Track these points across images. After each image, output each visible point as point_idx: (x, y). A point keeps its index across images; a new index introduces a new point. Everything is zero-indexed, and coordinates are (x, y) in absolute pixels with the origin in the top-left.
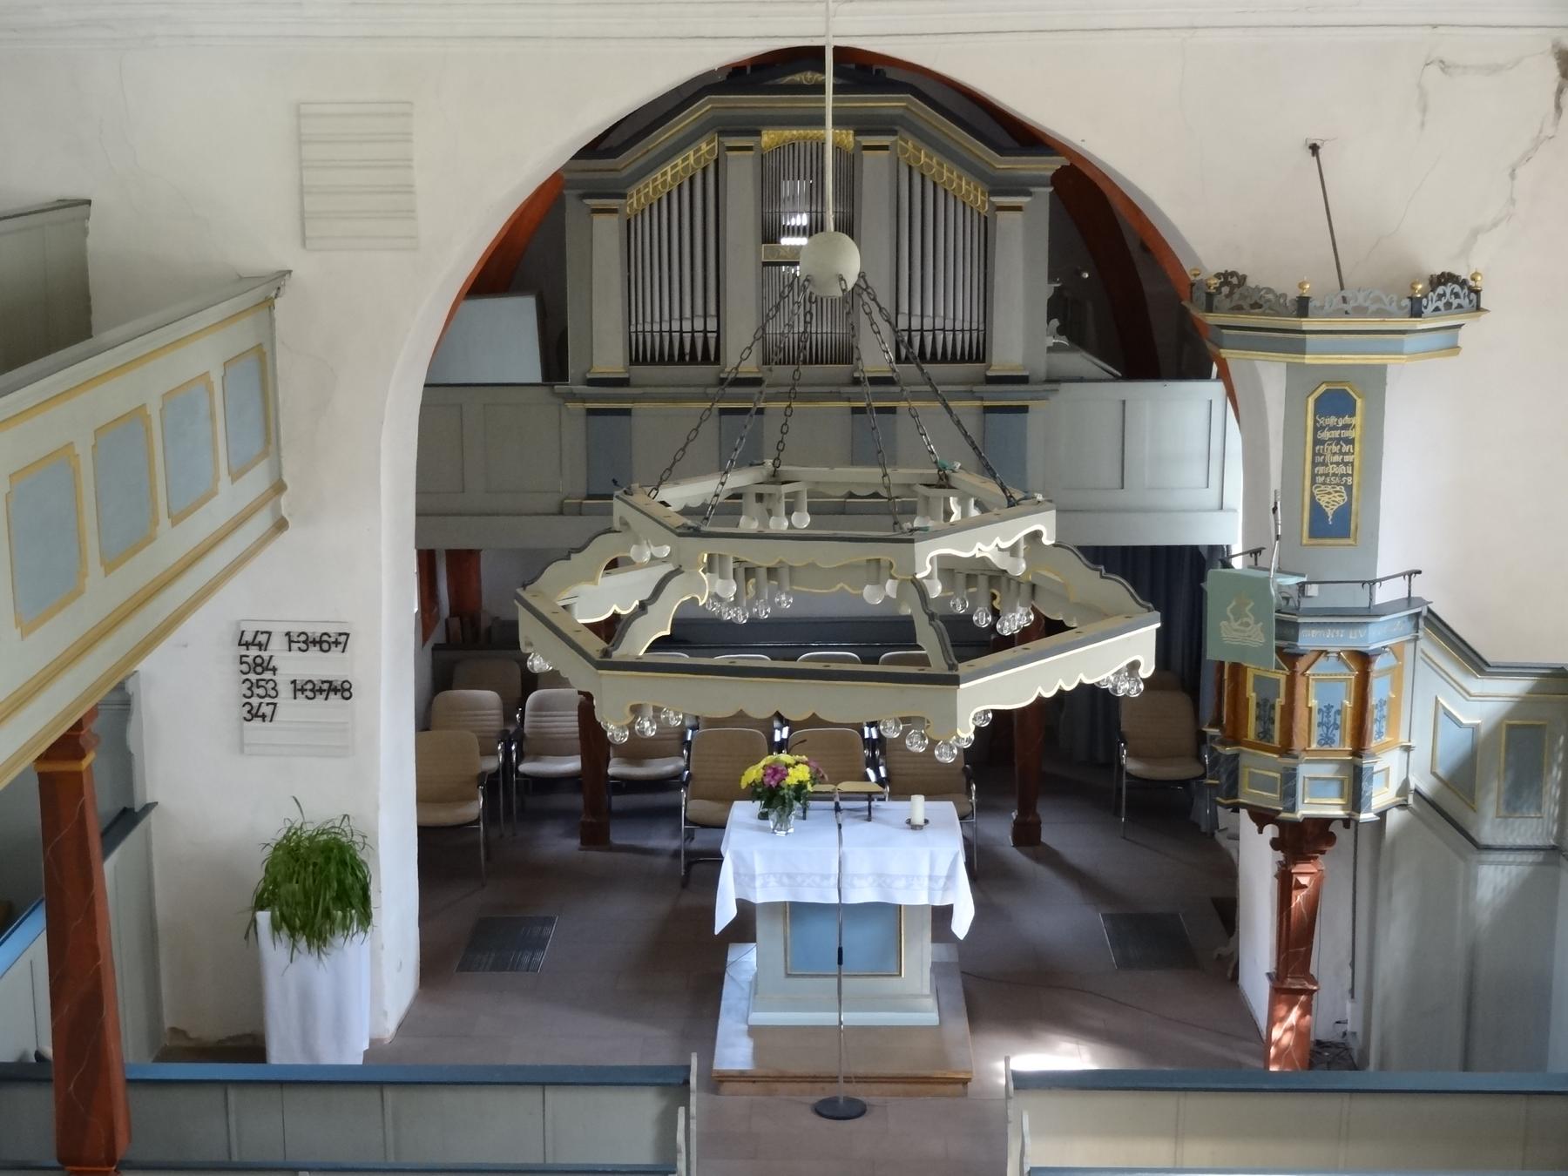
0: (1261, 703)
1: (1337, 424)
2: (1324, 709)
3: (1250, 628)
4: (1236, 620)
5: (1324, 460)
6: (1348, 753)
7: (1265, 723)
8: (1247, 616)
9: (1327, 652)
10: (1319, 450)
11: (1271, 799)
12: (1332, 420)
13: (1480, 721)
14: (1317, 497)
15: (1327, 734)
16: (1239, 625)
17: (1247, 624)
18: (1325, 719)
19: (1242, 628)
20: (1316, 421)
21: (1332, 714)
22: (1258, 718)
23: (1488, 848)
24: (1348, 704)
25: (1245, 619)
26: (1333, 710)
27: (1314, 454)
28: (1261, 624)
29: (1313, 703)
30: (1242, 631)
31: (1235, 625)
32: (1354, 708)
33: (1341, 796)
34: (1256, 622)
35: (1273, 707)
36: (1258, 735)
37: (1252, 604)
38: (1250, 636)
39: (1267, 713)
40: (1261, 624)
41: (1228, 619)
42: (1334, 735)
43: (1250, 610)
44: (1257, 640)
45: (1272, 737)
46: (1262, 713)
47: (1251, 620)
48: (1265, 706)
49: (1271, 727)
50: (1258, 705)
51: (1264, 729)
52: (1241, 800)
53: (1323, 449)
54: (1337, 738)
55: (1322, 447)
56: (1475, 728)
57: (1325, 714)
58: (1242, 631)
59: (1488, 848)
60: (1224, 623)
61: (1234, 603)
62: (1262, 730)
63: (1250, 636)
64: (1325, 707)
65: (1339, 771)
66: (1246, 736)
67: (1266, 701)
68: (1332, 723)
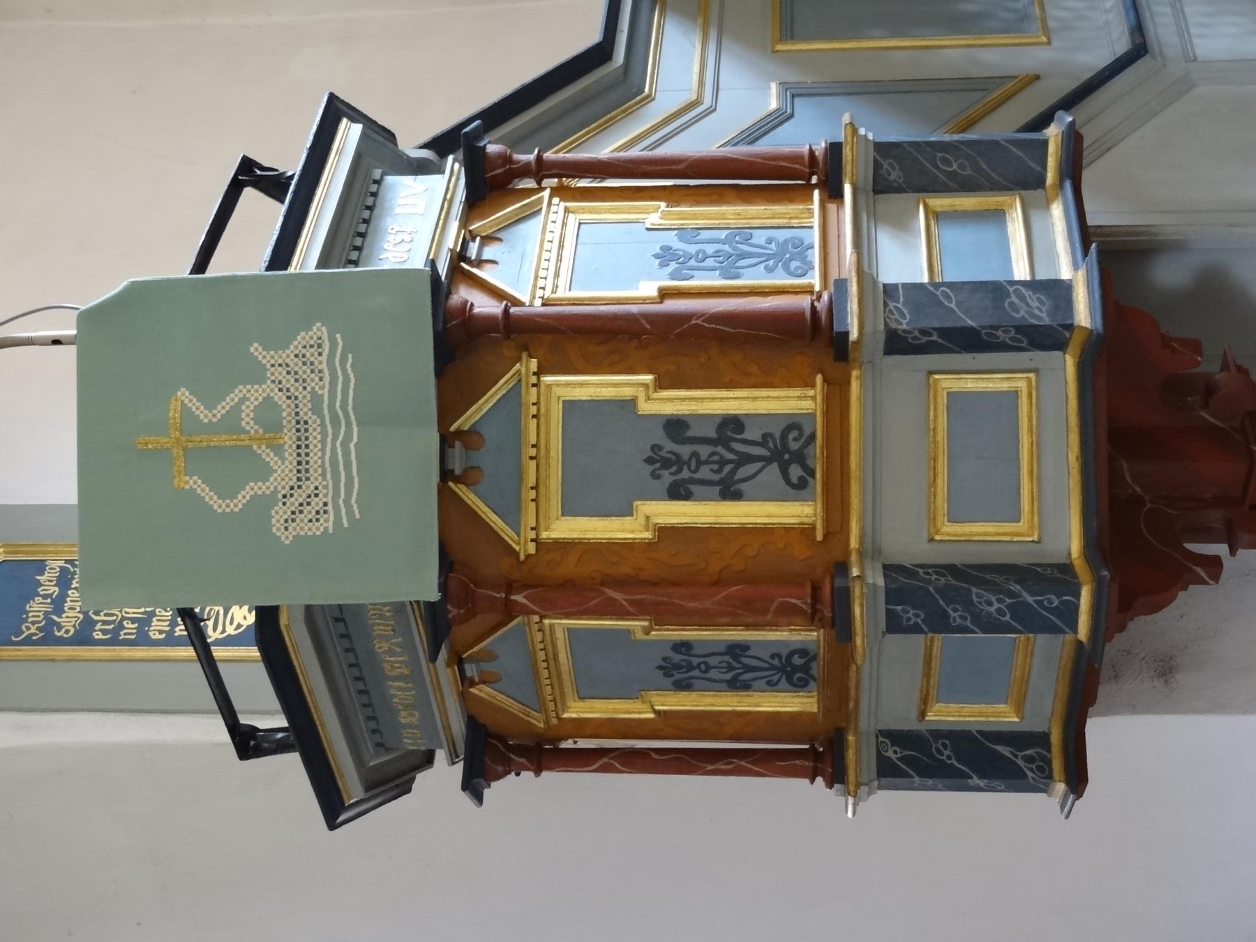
0: (667, 478)
1: (45, 597)
2: (673, 265)
3: (280, 398)
4: (264, 472)
5: (133, 620)
6: (832, 207)
7: (747, 459)
8: (236, 409)
9: (460, 256)
10: (104, 632)
11: (1039, 406)
12: (37, 608)
13: (774, 86)
14: (231, 630)
15: (770, 257)
16: (278, 449)
17: (268, 415)
18: (710, 262)
19: (288, 438)
20: (28, 642)
21: (692, 249)
22: (730, 492)
23: (1138, 29)
24: (655, 213)
25: (247, 419)
26: (677, 244)
27: (114, 641)
28: (255, 349)
29: (649, 289)
30: (301, 447)
31: (283, 470)
32: (672, 196)
33: (998, 216)
34: (256, 374)
35: (676, 426)
36: (799, 488)
37: (184, 394)
38: (316, 400)
39: (704, 451)
40: (255, 349)
41: (263, 504)
42: (769, 241)
43: (210, 407)
44: (324, 367)
45: (793, 425)
46: (705, 473)
47: (255, 394)
48: (674, 462)
49: (752, 433)
50: (678, 492)
51: (768, 461)
52: (1076, 547)
53: (105, 623)
54: (782, 235)
55: (98, 627)
56: (793, 92)
57: (693, 262)
58: (301, 447)
59: (1138, 29)
60: (279, 514)
61: (194, 483)
62: (775, 466)
63: (316, 400)
64: (663, 265)
65: (902, 223)
66: (806, 531)
67: (658, 461)
68: (726, 248)
